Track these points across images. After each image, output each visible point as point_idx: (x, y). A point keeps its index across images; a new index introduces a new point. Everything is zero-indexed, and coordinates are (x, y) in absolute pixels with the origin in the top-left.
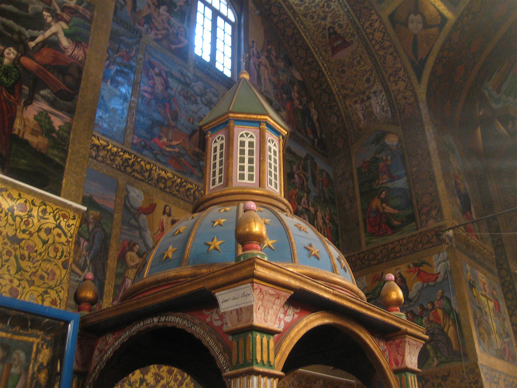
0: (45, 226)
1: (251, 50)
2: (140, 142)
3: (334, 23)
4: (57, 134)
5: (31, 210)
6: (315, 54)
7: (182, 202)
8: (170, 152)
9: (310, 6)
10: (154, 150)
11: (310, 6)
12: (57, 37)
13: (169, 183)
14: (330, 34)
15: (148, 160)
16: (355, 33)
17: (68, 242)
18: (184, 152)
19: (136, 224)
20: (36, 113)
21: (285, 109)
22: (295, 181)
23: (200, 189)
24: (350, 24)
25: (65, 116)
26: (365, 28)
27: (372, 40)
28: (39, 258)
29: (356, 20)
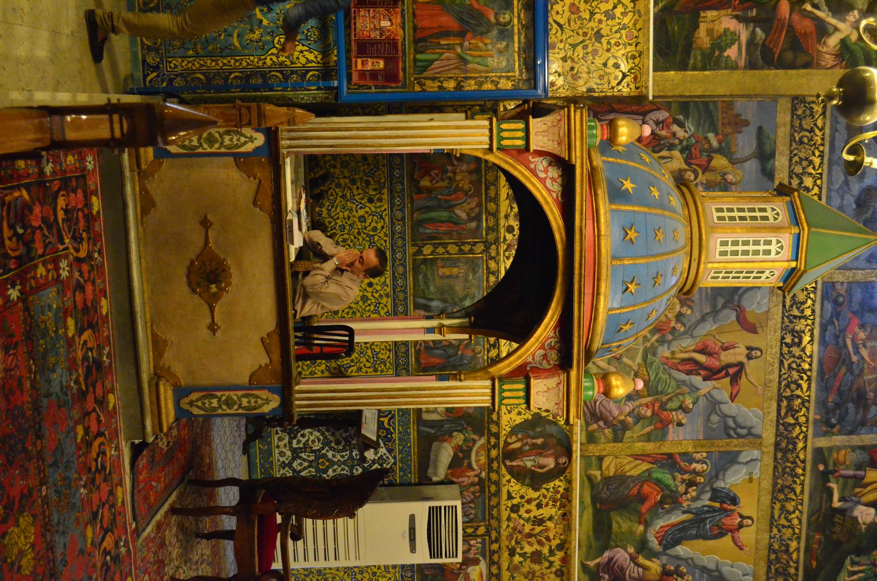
0: (620, 62)
2: (842, 295)
4: (720, 56)
5: (630, 45)
7: (775, 376)
8: (845, 345)
10: (838, 320)
12: (834, 32)
13: (796, 351)
17: (613, 88)
18: (857, 372)
19: (719, 306)
20: (732, 29)
23: (807, 404)
25: (743, 60)
28: (589, 62)
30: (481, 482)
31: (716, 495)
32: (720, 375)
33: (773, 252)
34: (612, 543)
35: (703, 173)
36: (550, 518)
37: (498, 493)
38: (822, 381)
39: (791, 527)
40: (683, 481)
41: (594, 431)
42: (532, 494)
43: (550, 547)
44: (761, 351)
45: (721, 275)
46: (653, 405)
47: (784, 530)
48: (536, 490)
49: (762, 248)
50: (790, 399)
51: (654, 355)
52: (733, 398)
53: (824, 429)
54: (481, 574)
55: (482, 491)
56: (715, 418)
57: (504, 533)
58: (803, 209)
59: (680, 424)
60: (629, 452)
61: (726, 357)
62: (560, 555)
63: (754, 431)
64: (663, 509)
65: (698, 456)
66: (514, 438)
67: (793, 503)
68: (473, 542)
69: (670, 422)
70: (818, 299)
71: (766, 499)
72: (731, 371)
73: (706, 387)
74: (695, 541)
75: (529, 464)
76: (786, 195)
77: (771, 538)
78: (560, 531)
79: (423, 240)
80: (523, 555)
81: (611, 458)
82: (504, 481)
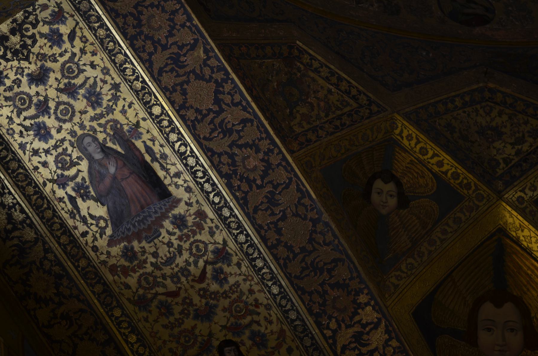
3: (237, 329)
9: (158, 273)
11: (158, 273)
26: (339, 350)
29: (310, 321)
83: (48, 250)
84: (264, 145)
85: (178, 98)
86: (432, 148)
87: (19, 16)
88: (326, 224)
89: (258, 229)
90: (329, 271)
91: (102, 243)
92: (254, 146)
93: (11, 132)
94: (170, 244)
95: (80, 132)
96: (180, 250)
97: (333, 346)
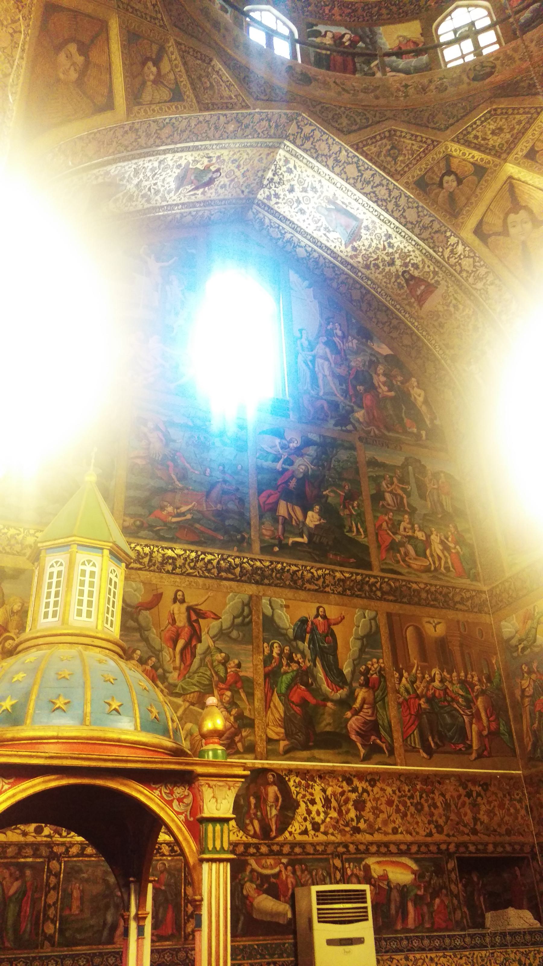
1: (299, 343)
2: (134, 522)
3: (406, 265)
6: (397, 312)
7: (200, 581)
13: (179, 562)
14: (407, 281)
15: (143, 542)
16: (437, 269)
18: (199, 516)
21: (361, 407)
22: (385, 503)
23: (225, 556)
24: (426, 260)
27: (461, 271)
29: (431, 251)
30: (292, 863)
31: (299, 636)
32: (197, 628)
33: (93, 569)
34: (344, 731)
35: (8, 632)
36: (324, 791)
37: (302, 845)
38: (205, 543)
39: (324, 576)
40: (288, 665)
41: (243, 746)
42: (302, 809)
43: (349, 791)
44: (178, 591)
45: (110, 618)
46: (222, 689)
47: (327, 582)
48: (298, 805)
49: (87, 579)
50: (220, 569)
51: (176, 686)
52: (217, 618)
53: (245, 544)
54: (378, 863)
55: (300, 862)
56: (234, 634)
57: (338, 838)
58: (55, 540)
59: (239, 666)
60: (263, 714)
61: (181, 621)
62: (356, 782)
63: (246, 601)
64: (312, 684)
65: (267, 651)
66: (250, 828)
67: (305, 573)
68: (349, 872)
69: (236, 674)
70: (136, 541)
71: (303, 594)
72: (194, 617)
73: (207, 641)
74: (339, 656)
75: (274, 812)
76: (39, 554)
77: (333, 593)
78: (335, 781)
79: (37, 934)
80: (359, 818)
81: (268, 730)
82: (290, 838)
83: (325, 258)
84: (385, 182)
85: (344, 176)
86: (467, 151)
87: (273, 167)
88: (422, 207)
89: (396, 219)
90: (431, 227)
91: (343, 248)
92: (381, 184)
93: (291, 216)
94: (367, 239)
95: (316, 206)
96: (372, 240)
97: (444, 259)
